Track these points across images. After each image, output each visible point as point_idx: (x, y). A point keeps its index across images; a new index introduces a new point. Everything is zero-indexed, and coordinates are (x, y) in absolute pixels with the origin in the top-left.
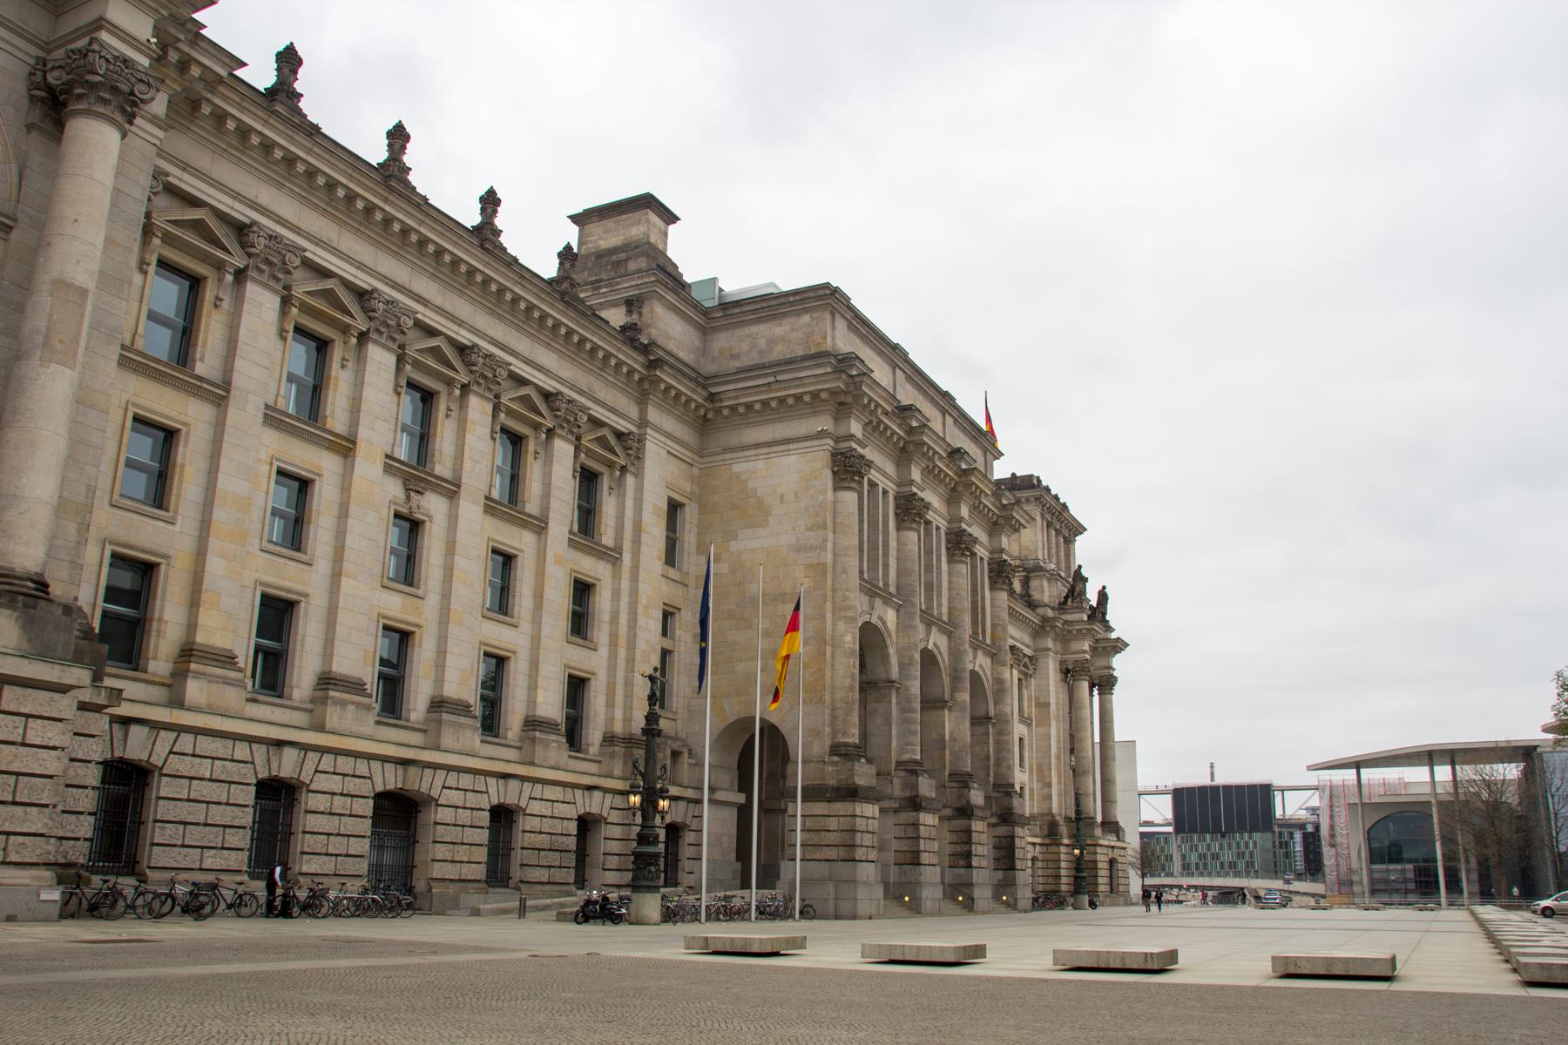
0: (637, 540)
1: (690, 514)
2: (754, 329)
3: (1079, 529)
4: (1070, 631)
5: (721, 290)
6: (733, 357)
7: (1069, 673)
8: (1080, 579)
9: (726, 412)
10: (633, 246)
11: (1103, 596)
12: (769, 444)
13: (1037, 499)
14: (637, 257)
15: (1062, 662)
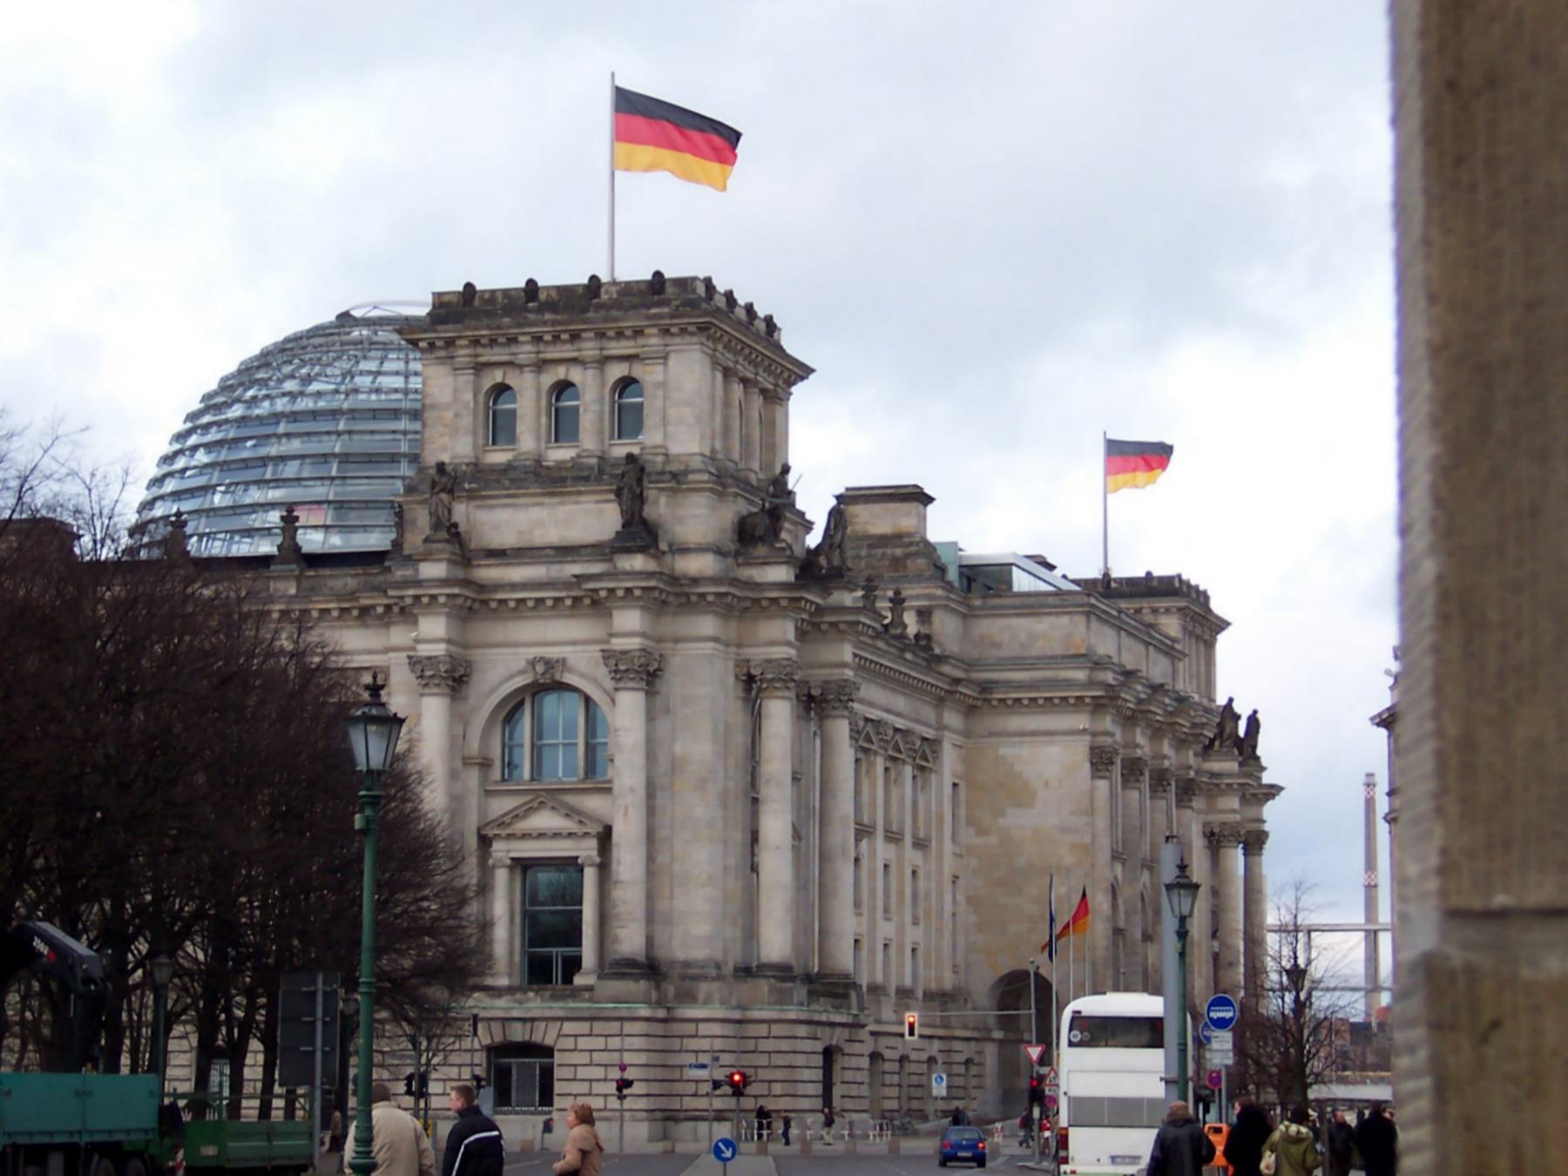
0: (940, 829)
1: (962, 788)
2: (1015, 622)
3: (1222, 625)
4: (1217, 785)
5: (961, 550)
6: (997, 645)
7: (1215, 840)
8: (1229, 712)
9: (995, 703)
10: (906, 540)
11: (1254, 722)
12: (1034, 733)
13: (1180, 610)
14: (917, 554)
15: (1205, 824)
